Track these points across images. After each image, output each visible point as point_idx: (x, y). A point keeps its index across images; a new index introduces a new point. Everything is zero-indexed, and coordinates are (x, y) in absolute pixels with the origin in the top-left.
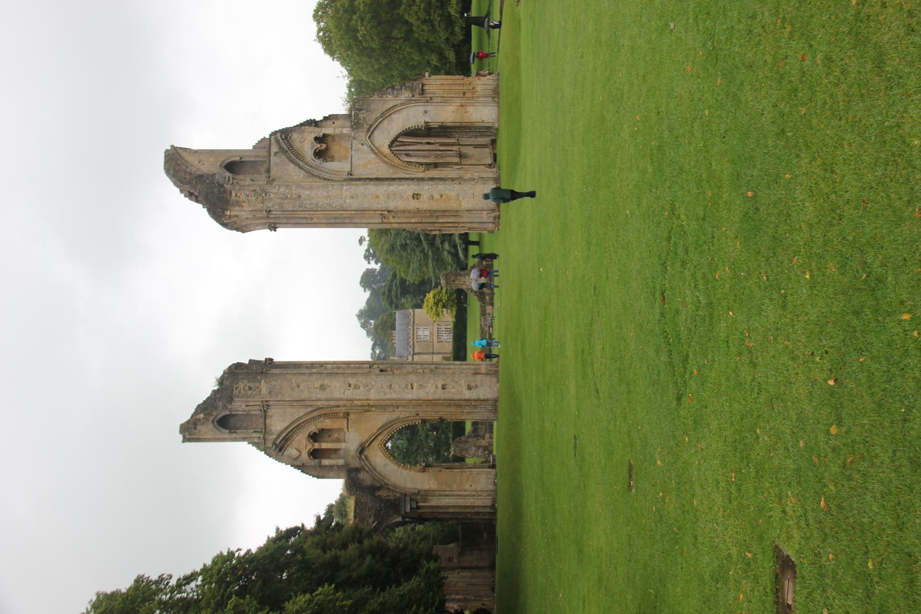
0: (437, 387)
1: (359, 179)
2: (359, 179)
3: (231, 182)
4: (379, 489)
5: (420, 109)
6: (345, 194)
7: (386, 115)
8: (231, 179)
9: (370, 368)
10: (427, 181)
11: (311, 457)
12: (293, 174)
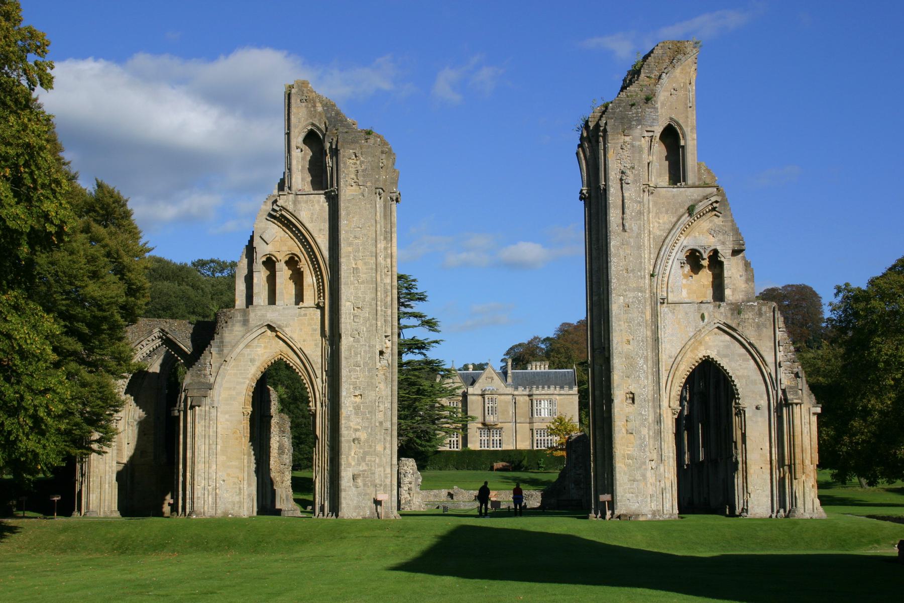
0: (356, 430)
1: (655, 314)
2: (655, 314)
3: (646, 134)
4: (221, 351)
5: (764, 403)
6: (631, 295)
7: (751, 350)
8: (651, 134)
9: (386, 337)
10: (655, 413)
11: (264, 259)
12: (661, 221)
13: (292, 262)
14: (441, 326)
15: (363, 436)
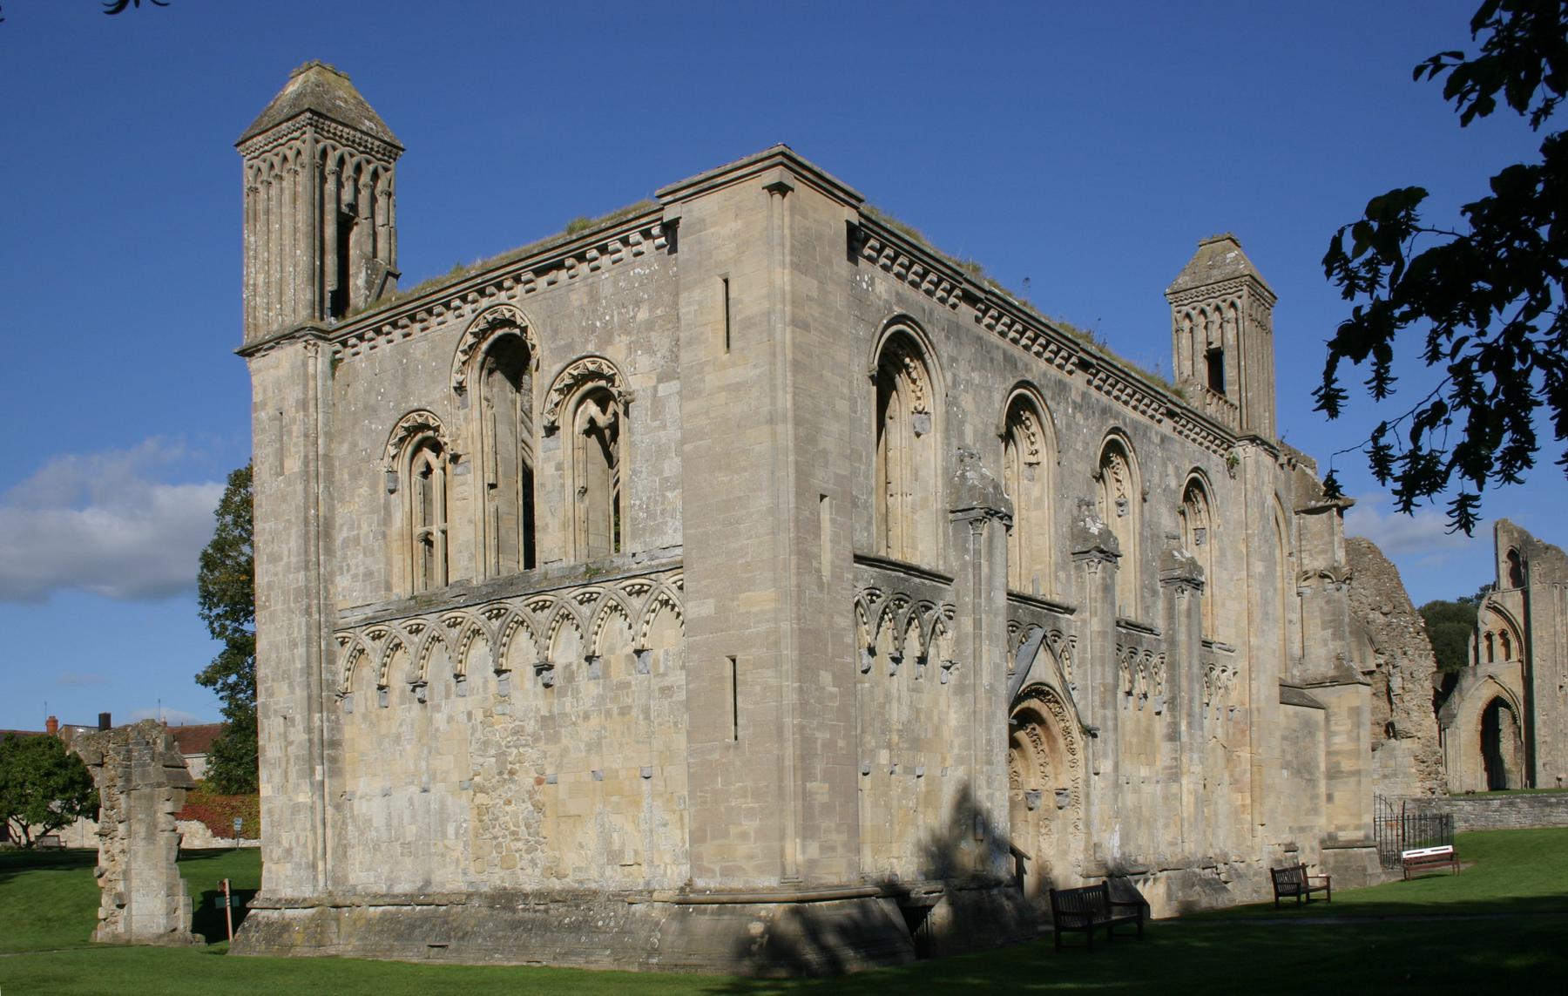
4: (1460, 694)
13: (1503, 634)
15: (1548, 739)
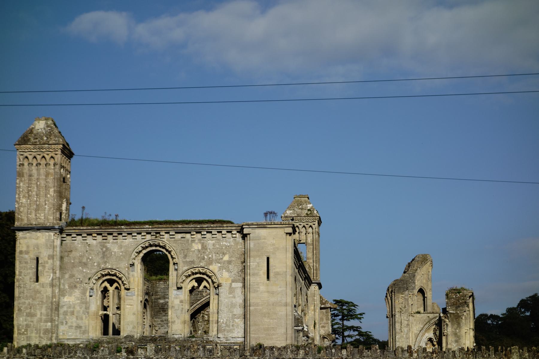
3: (411, 293)
8: (412, 293)
12: (417, 327)
14: (372, 332)
